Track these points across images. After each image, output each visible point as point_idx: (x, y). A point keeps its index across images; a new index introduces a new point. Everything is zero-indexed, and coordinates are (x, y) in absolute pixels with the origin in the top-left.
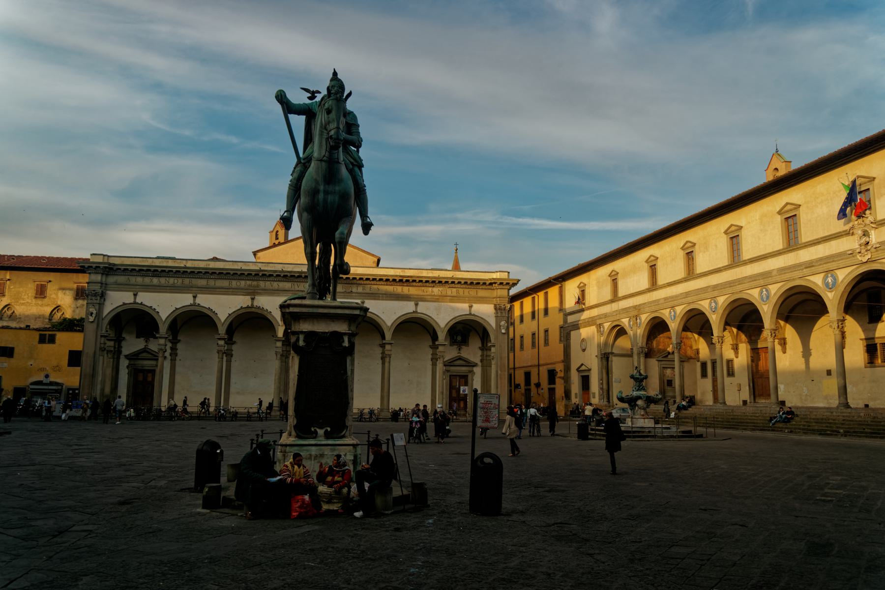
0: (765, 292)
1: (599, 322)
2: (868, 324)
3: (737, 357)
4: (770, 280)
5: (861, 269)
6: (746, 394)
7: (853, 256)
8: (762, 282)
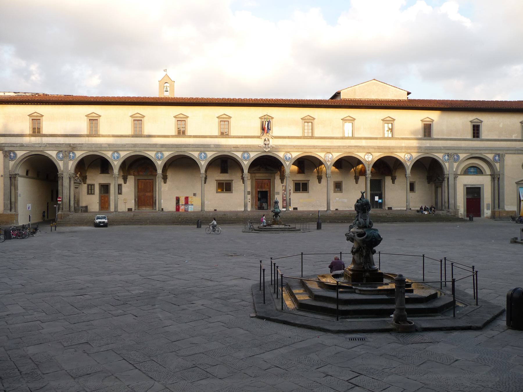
0: (203, 154)
1: (6, 149)
2: (220, 174)
3: (125, 183)
4: (208, 149)
5: (262, 154)
6: (131, 204)
7: (261, 148)
8: (202, 149)
